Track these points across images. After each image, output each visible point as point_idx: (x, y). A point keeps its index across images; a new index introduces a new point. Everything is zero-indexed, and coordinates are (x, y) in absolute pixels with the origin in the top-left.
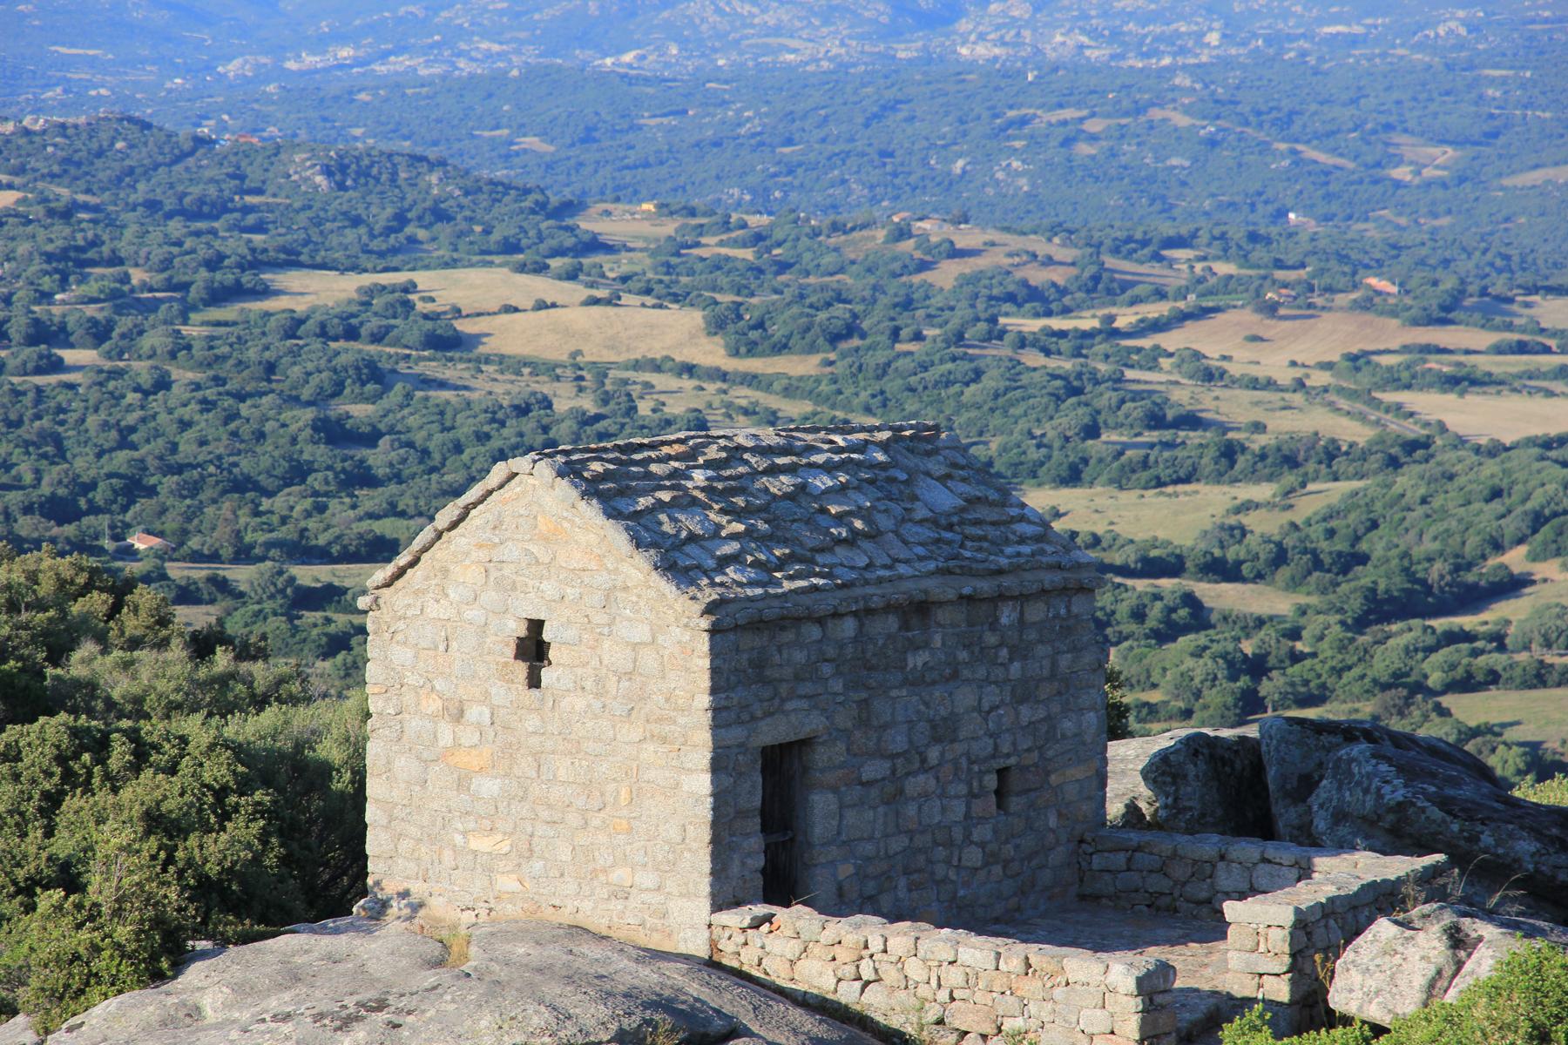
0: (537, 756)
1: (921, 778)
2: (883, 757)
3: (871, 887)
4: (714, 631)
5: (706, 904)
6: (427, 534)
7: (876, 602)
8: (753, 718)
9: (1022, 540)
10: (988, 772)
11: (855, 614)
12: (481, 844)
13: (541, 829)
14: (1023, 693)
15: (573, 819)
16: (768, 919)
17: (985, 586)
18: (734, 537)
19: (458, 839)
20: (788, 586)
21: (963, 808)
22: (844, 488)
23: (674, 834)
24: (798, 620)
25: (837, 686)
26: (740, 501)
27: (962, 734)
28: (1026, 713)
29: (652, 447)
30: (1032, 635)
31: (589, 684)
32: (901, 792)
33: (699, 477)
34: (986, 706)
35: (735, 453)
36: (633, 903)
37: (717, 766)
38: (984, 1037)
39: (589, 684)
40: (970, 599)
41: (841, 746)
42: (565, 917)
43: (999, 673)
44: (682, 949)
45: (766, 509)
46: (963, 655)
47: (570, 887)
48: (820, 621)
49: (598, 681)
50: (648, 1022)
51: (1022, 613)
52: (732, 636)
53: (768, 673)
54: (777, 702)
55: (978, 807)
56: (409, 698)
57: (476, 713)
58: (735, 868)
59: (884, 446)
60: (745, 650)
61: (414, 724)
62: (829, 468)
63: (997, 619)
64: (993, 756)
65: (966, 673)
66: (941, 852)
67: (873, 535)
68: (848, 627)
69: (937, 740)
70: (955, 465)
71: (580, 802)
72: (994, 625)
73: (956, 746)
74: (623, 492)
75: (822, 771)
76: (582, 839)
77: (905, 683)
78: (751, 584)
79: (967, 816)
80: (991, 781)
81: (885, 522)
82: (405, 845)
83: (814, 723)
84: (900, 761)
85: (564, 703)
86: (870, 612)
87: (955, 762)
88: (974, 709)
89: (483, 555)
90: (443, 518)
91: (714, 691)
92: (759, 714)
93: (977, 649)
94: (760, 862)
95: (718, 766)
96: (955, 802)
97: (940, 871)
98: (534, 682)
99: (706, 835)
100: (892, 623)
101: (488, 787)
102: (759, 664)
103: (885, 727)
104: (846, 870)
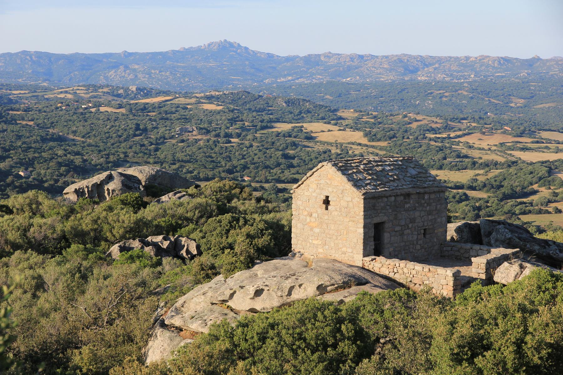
0: (327, 224)
1: (408, 230)
3: (396, 253)
4: (364, 199)
5: (362, 256)
6: (305, 178)
7: (399, 193)
8: (372, 217)
9: (430, 181)
11: (394, 196)
12: (315, 242)
13: (328, 239)
14: (430, 213)
15: (334, 237)
16: (375, 259)
17: (422, 191)
18: (369, 179)
19: (311, 241)
20: (380, 190)
22: (392, 169)
23: (356, 241)
24: (382, 197)
25: (390, 211)
26: (370, 172)
28: (430, 217)
29: (352, 160)
30: (432, 201)
31: (338, 209)
32: (403, 233)
33: (362, 167)
34: (422, 215)
35: (370, 162)
36: (346, 255)
38: (420, 285)
39: (338, 209)
41: (391, 223)
42: (333, 258)
43: (424, 209)
44: (357, 265)
45: (377, 173)
46: (417, 205)
47: (334, 252)
48: (387, 197)
49: (340, 209)
50: (349, 280)
56: (301, 212)
57: (315, 215)
58: (368, 248)
59: (401, 161)
60: (371, 203)
61: (302, 217)
62: (389, 165)
65: (418, 209)
66: (411, 246)
67: (398, 179)
68: (393, 198)
69: (411, 222)
70: (416, 165)
71: (336, 234)
72: (424, 199)
74: (346, 170)
76: (336, 242)
78: (372, 189)
79: (417, 239)
80: (422, 231)
81: (401, 177)
82: (300, 242)
83: (385, 219)
85: (333, 213)
86: (397, 195)
87: (415, 227)
89: (317, 182)
90: (308, 175)
91: (364, 211)
94: (373, 247)
95: (365, 227)
97: (411, 250)
98: (327, 209)
99: (362, 241)
100: (402, 198)
101: (317, 230)
102: (374, 206)
103: (400, 220)
104: (391, 249)
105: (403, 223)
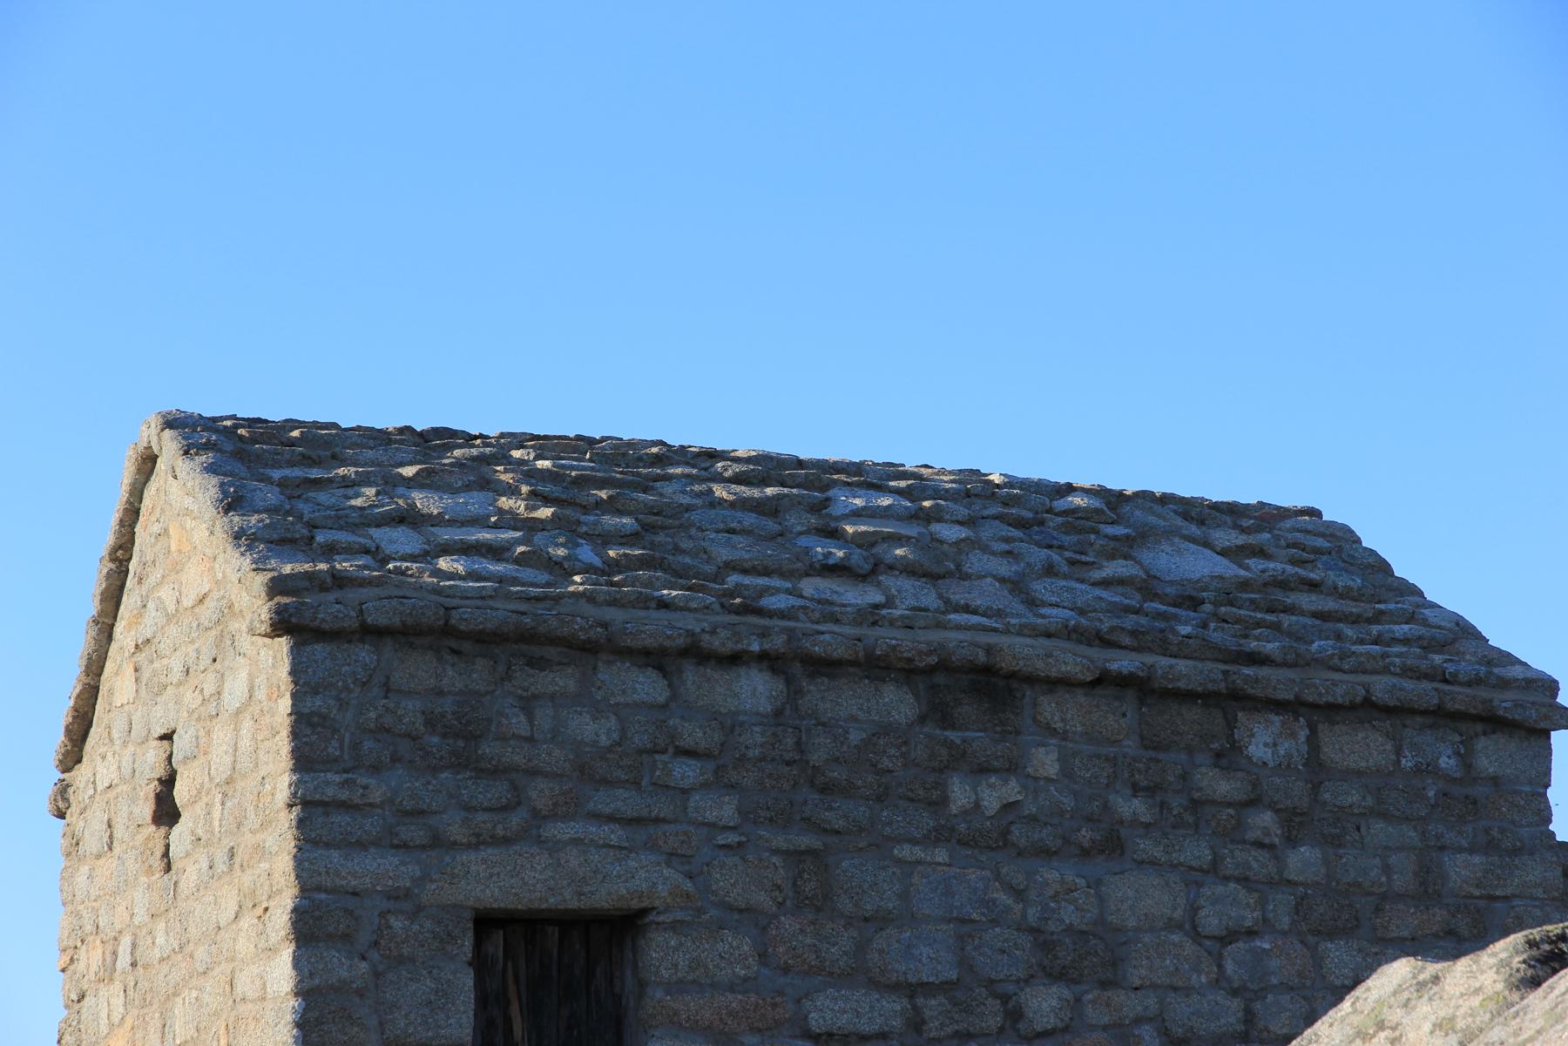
2: (874, 984)
7: (831, 640)
8: (437, 842)
24: (588, 650)
27: (1137, 973)
30: (1352, 797)
34: (1211, 921)
37: (309, 928)
40: (1139, 687)
43: (1258, 863)
46: (1131, 807)
48: (656, 659)
51: (1313, 741)
52: (364, 653)
53: (487, 749)
54: (516, 820)
63: (1236, 748)
68: (755, 690)
69: (1059, 976)
72: (1228, 756)
73: (1119, 997)
75: (677, 987)
84: (932, 1006)
88: (1172, 925)
92: (456, 830)
93: (1177, 803)
103: (881, 920)
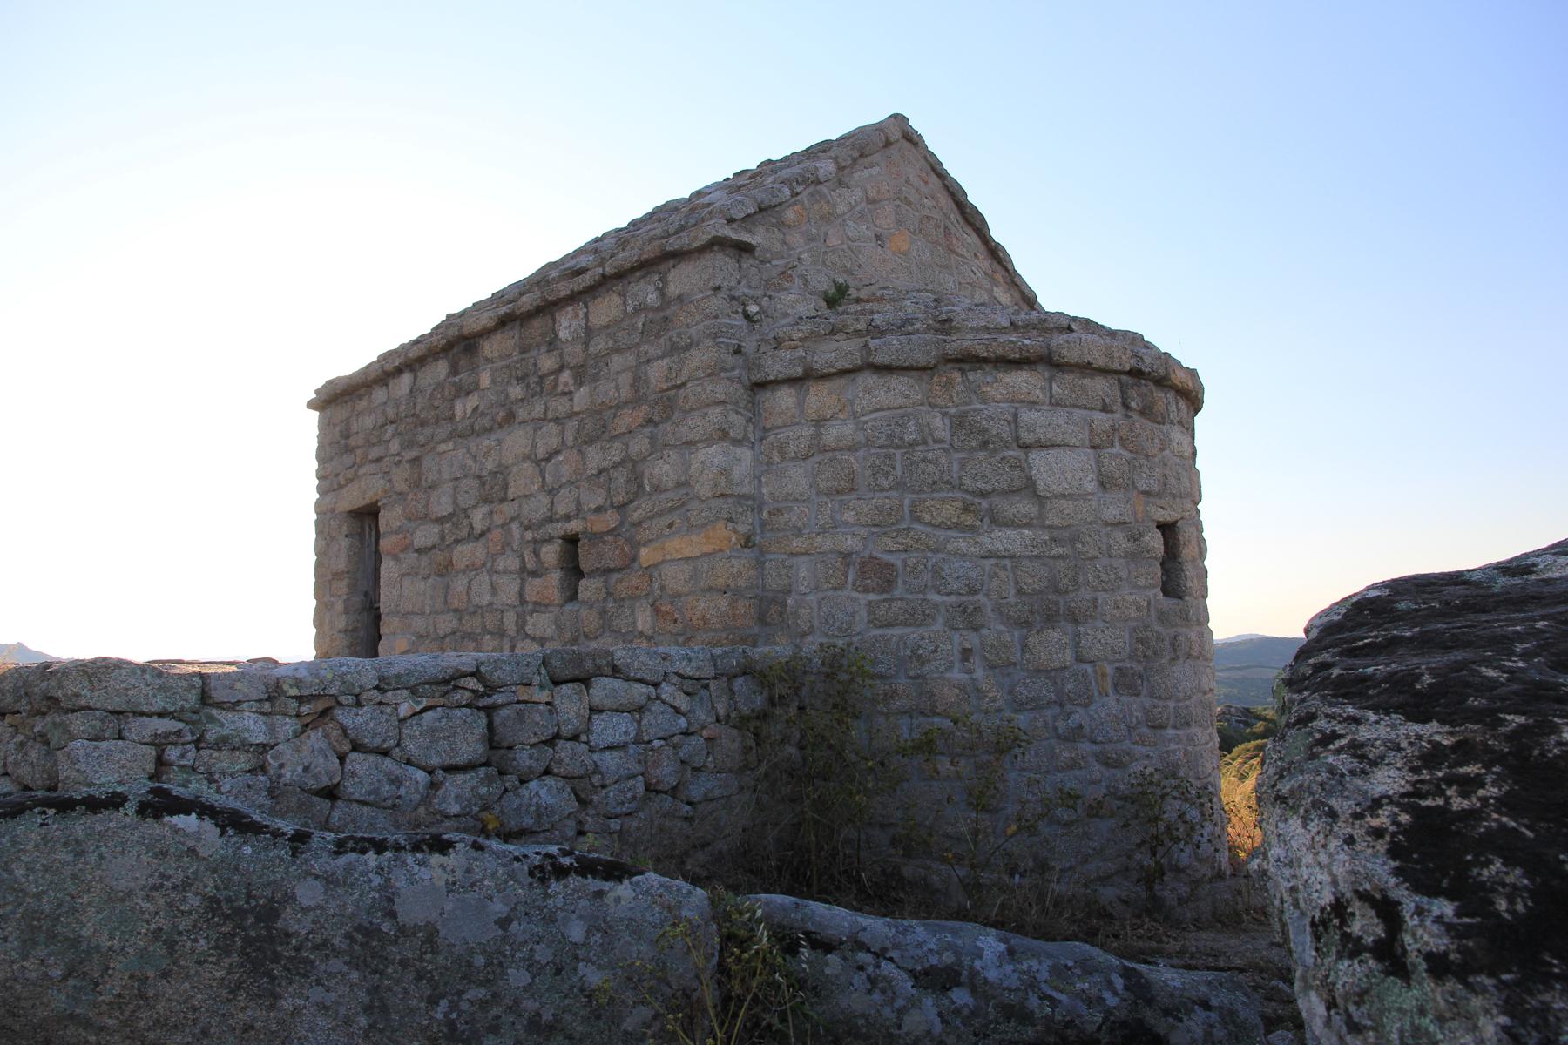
10: (550, 540)
14: (597, 427)
21: (515, 588)
25: (395, 446)
27: (511, 493)
28: (595, 457)
34: (541, 452)
43: (560, 406)
46: (516, 391)
55: (534, 588)
64: (550, 520)
65: (522, 413)
72: (552, 343)
77: (455, 435)
88: (526, 457)
93: (532, 380)
96: (505, 579)
105: (442, 504)
